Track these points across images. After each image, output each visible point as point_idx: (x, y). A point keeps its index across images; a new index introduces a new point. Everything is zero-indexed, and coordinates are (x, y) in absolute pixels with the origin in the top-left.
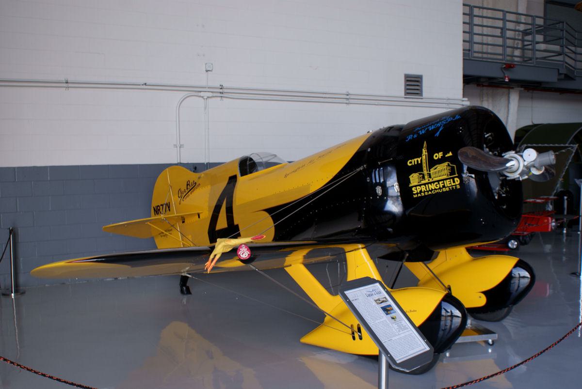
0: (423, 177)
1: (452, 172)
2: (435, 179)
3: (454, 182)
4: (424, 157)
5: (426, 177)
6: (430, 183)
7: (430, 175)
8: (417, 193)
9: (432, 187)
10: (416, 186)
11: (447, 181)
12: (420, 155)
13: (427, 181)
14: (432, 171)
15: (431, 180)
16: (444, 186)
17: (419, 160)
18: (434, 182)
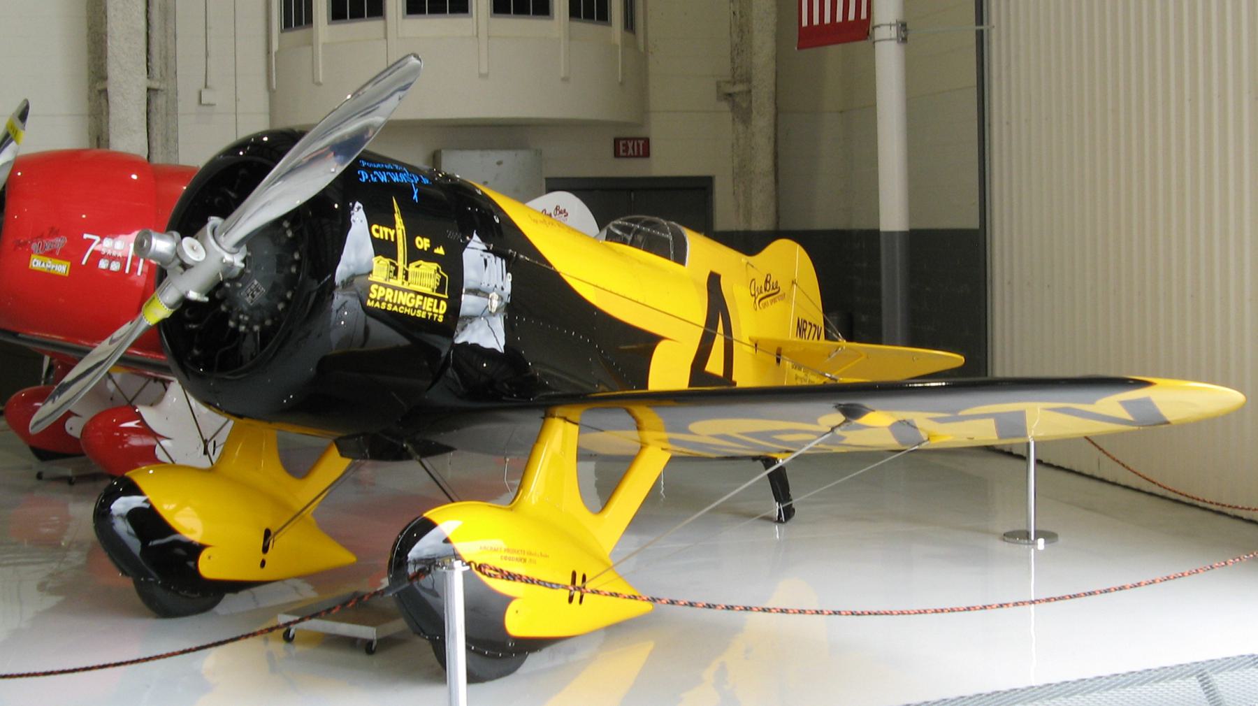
0: (396, 273)
1: (440, 289)
2: (412, 287)
3: (438, 307)
4: (400, 233)
5: (400, 273)
6: (404, 290)
7: (406, 274)
8: (376, 300)
9: (404, 298)
10: (380, 284)
11: (430, 300)
12: (392, 225)
13: (398, 282)
14: (412, 265)
15: (405, 286)
16: (420, 308)
17: (392, 233)
18: (409, 291)
